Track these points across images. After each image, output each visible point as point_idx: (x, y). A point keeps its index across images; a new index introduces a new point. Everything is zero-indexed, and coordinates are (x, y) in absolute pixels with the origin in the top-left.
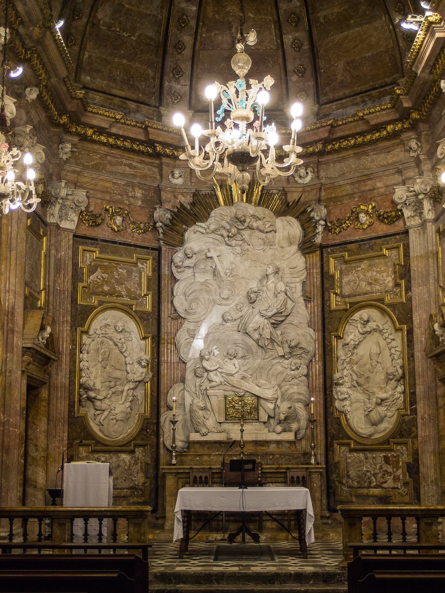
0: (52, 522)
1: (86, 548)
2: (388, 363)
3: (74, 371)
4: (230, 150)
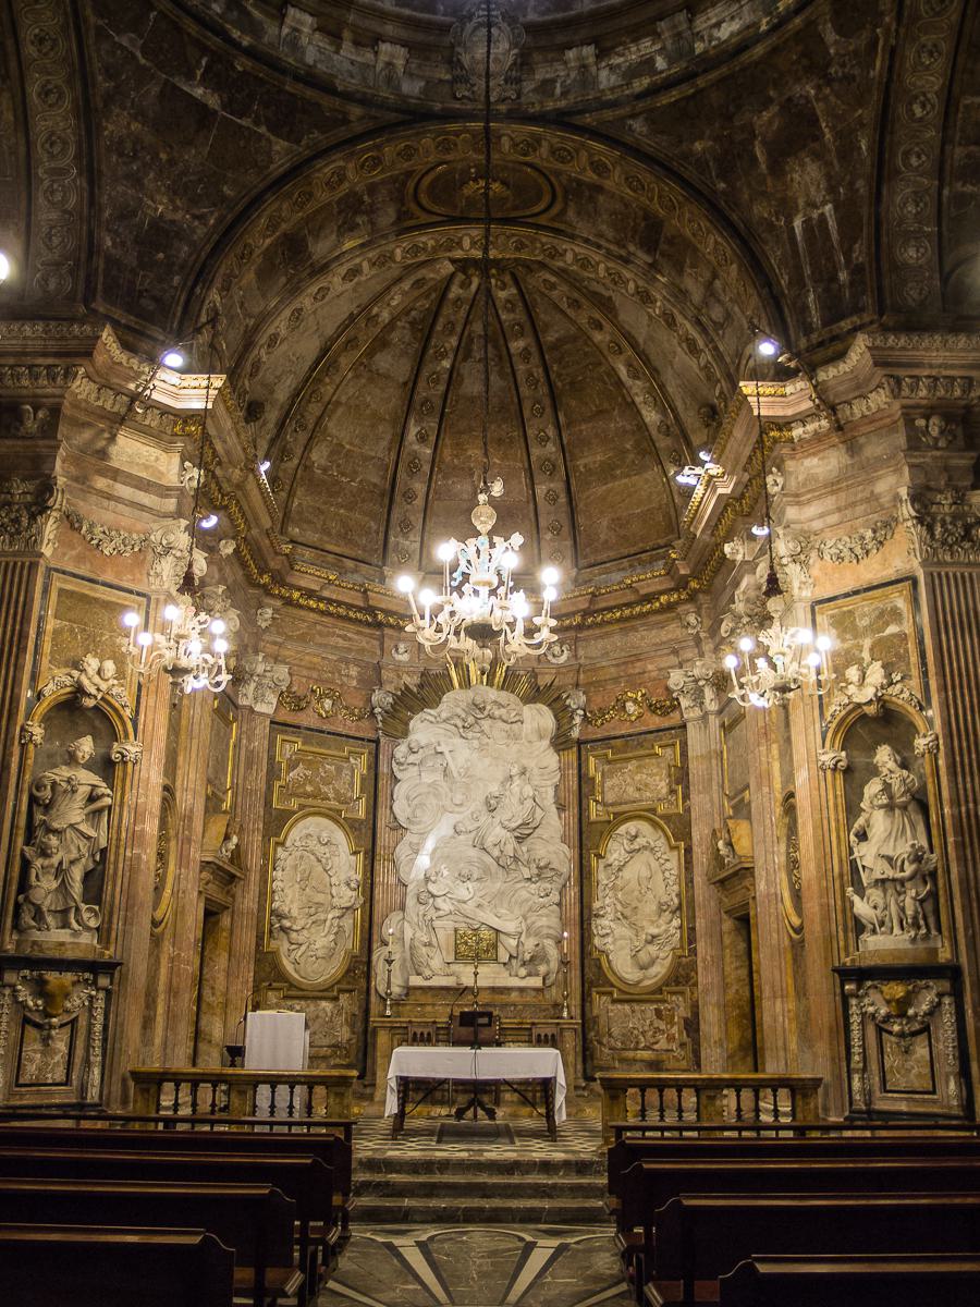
0: (229, 1089)
1: (272, 1124)
2: (661, 889)
3: (264, 894)
4: (468, 621)
